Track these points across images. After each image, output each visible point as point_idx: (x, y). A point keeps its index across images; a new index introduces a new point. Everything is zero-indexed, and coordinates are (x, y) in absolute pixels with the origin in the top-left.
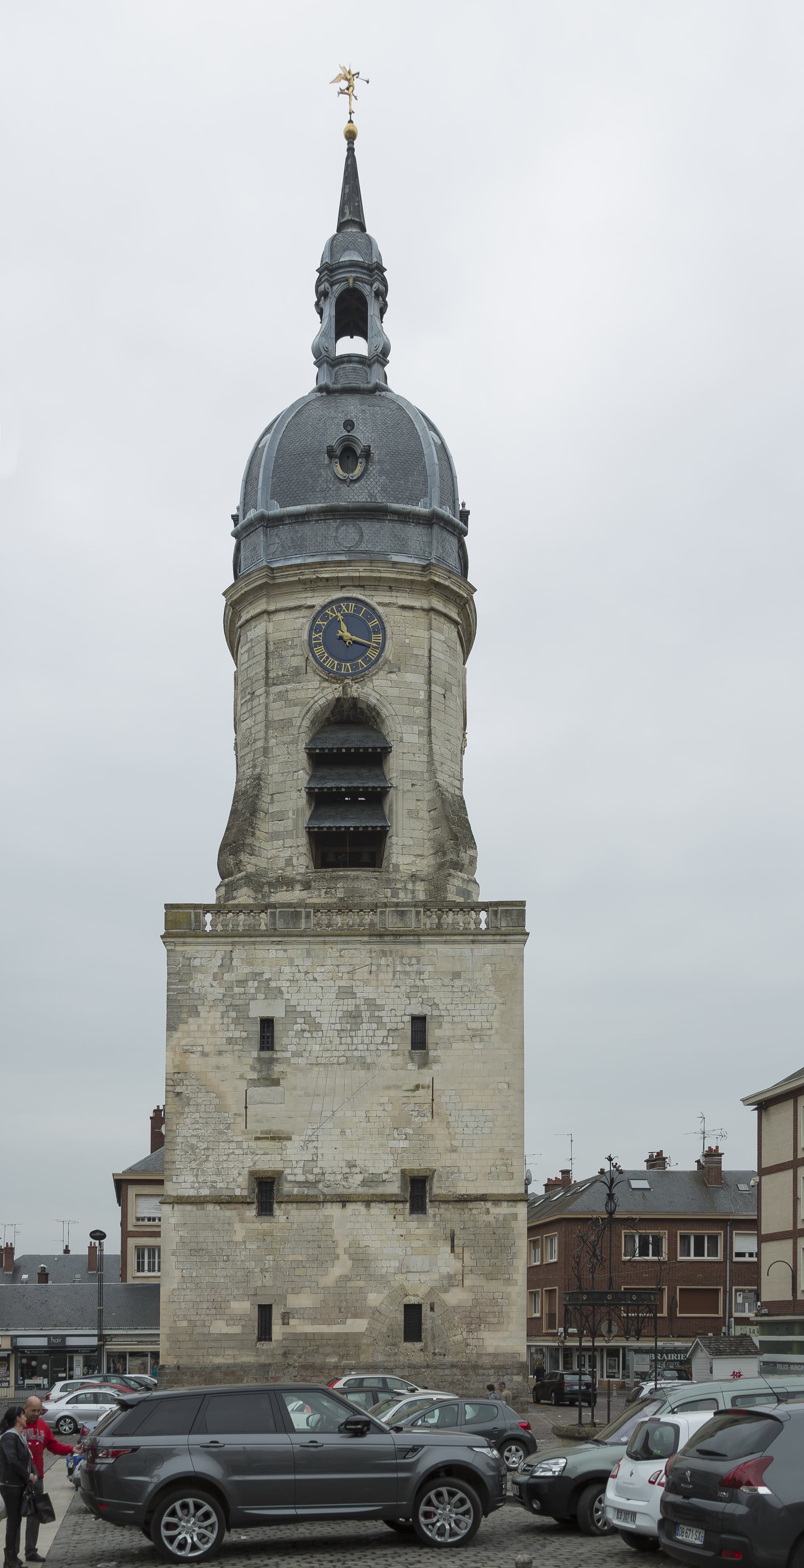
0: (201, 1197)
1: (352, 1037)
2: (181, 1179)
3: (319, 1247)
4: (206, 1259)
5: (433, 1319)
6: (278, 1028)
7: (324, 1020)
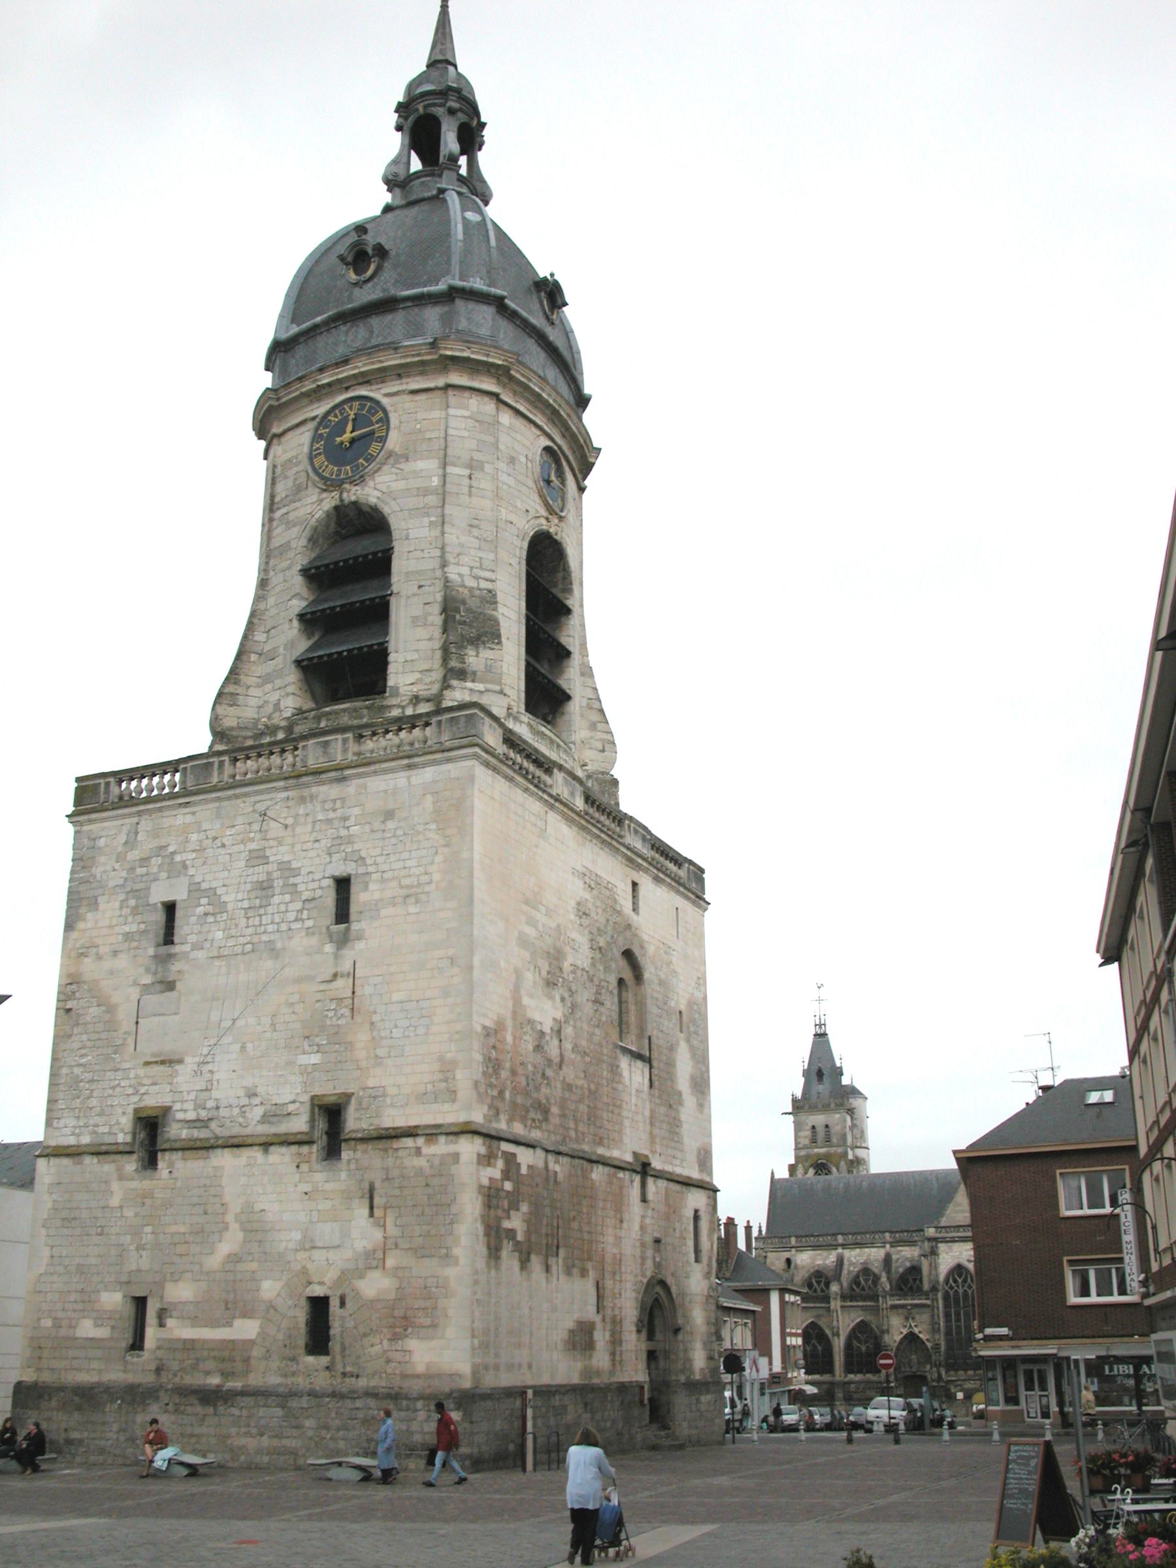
1: (260, 916)
2: (62, 1122)
3: (206, 1213)
4: (78, 1231)
5: (343, 1318)
6: (179, 913)
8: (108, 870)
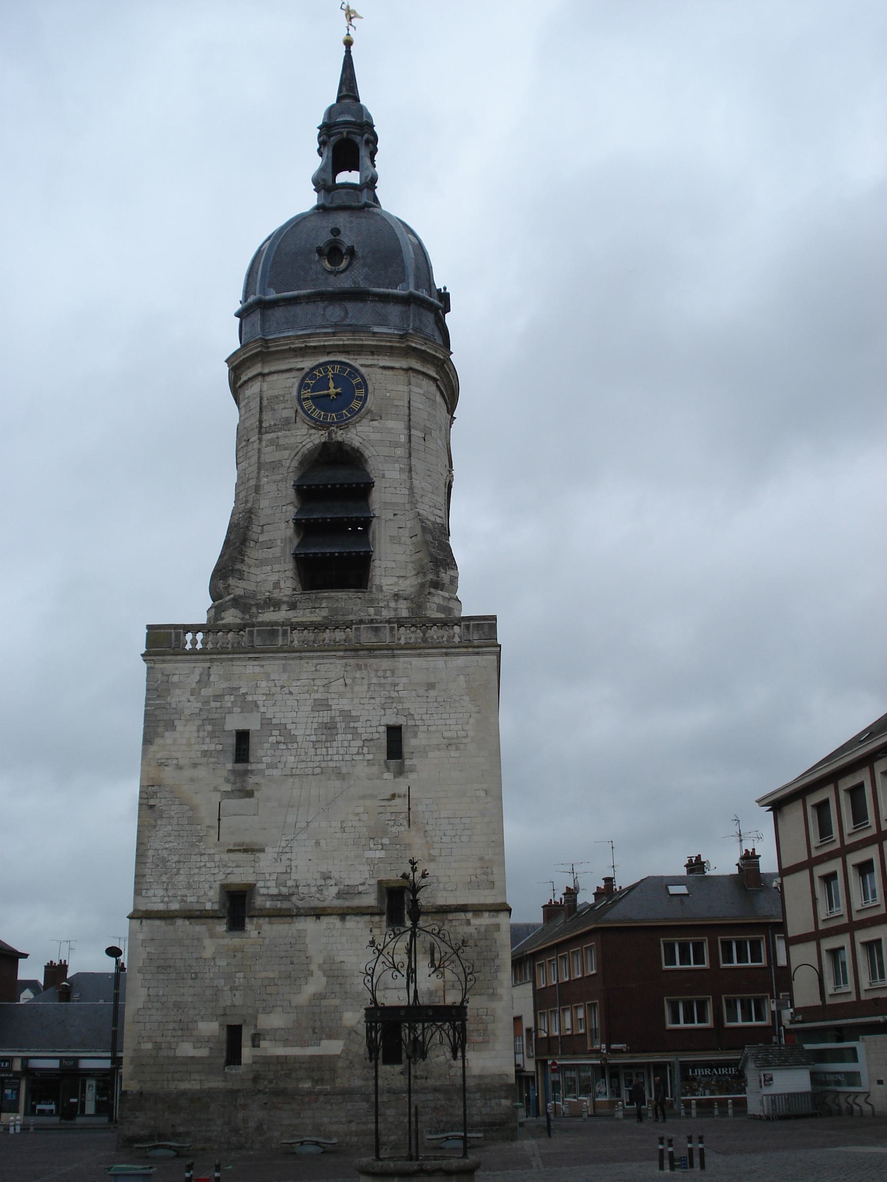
0: (171, 911)
1: (327, 748)
2: (151, 893)
3: (292, 963)
6: (253, 740)
7: (299, 732)
8: (179, 698)
